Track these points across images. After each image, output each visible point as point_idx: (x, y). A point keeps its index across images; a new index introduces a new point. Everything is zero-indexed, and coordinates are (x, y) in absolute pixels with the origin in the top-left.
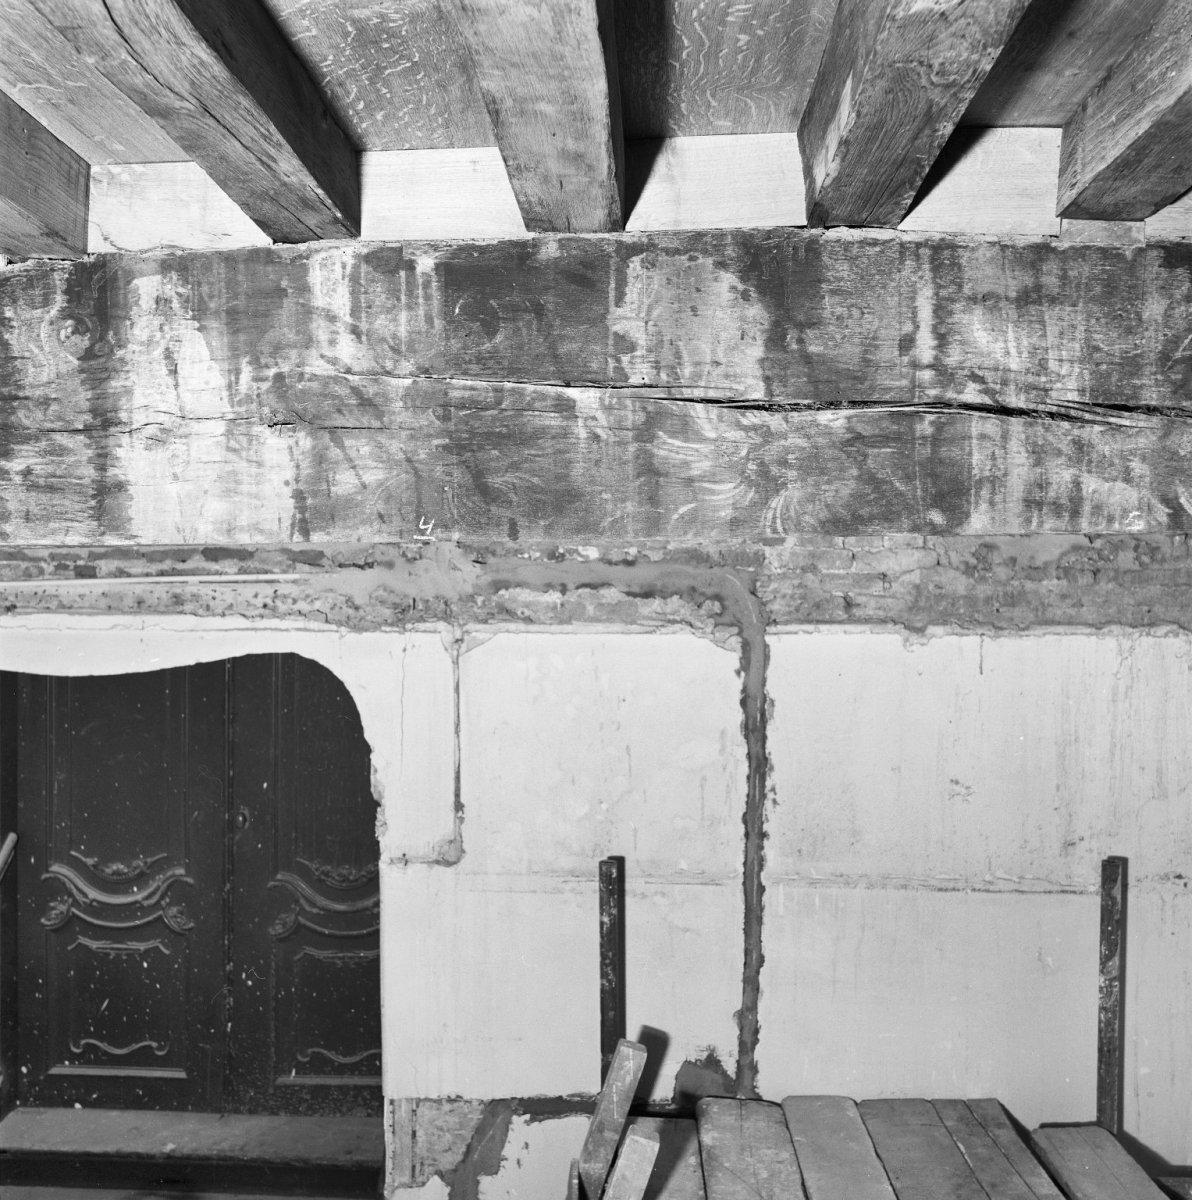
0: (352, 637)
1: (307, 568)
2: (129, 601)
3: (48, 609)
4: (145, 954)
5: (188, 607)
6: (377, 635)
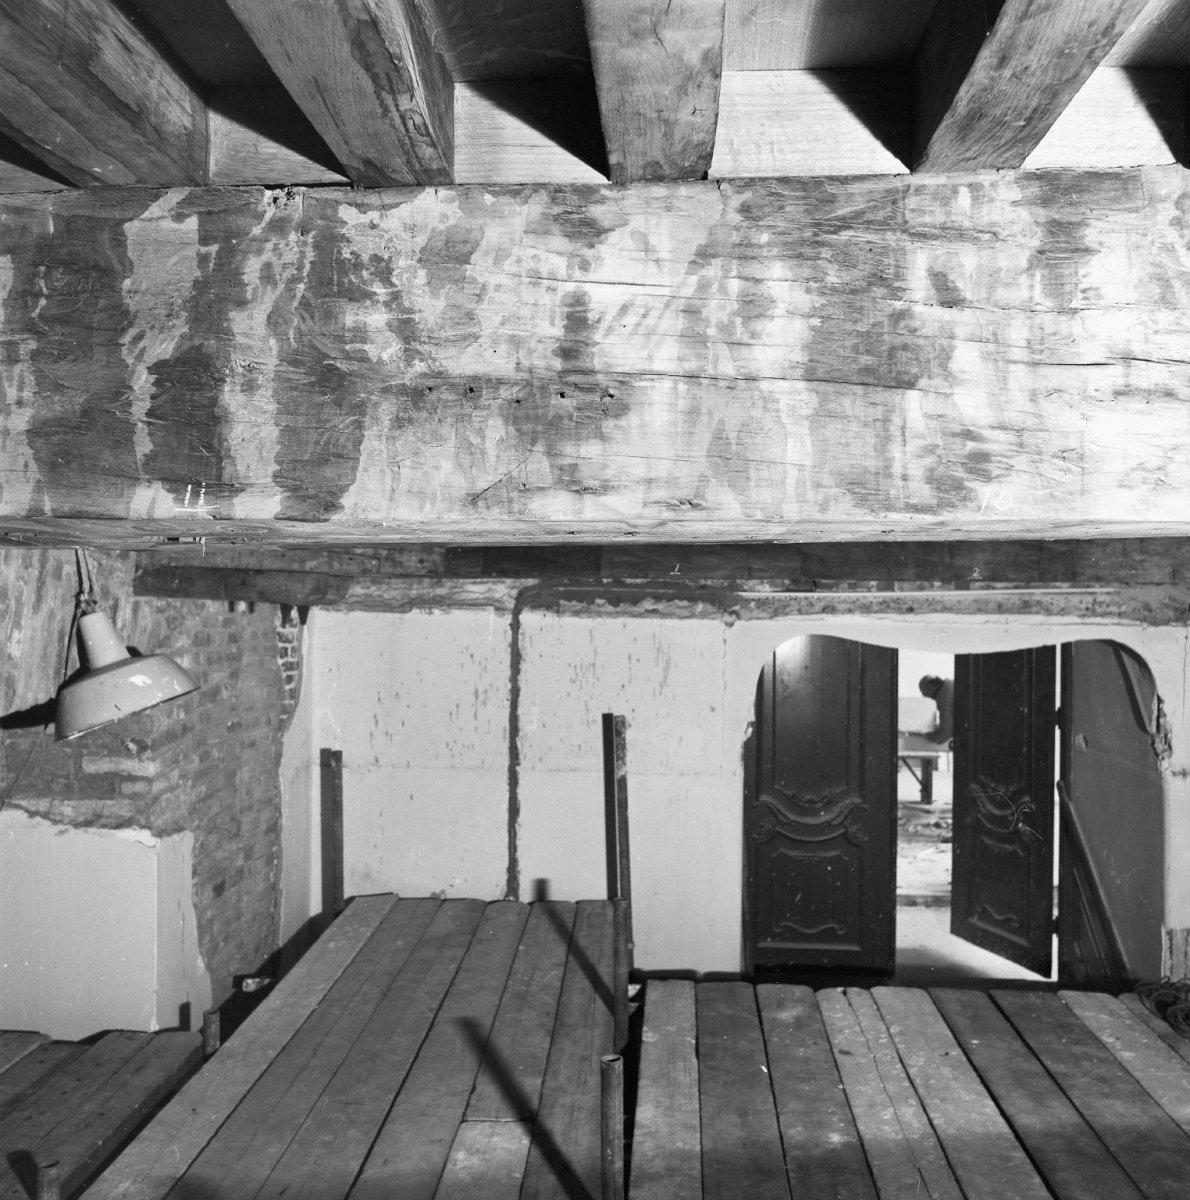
0: (1152, 629)
1: (1116, 584)
2: (991, 606)
3: (936, 611)
4: (830, 861)
5: (1034, 609)
6: (1168, 628)
